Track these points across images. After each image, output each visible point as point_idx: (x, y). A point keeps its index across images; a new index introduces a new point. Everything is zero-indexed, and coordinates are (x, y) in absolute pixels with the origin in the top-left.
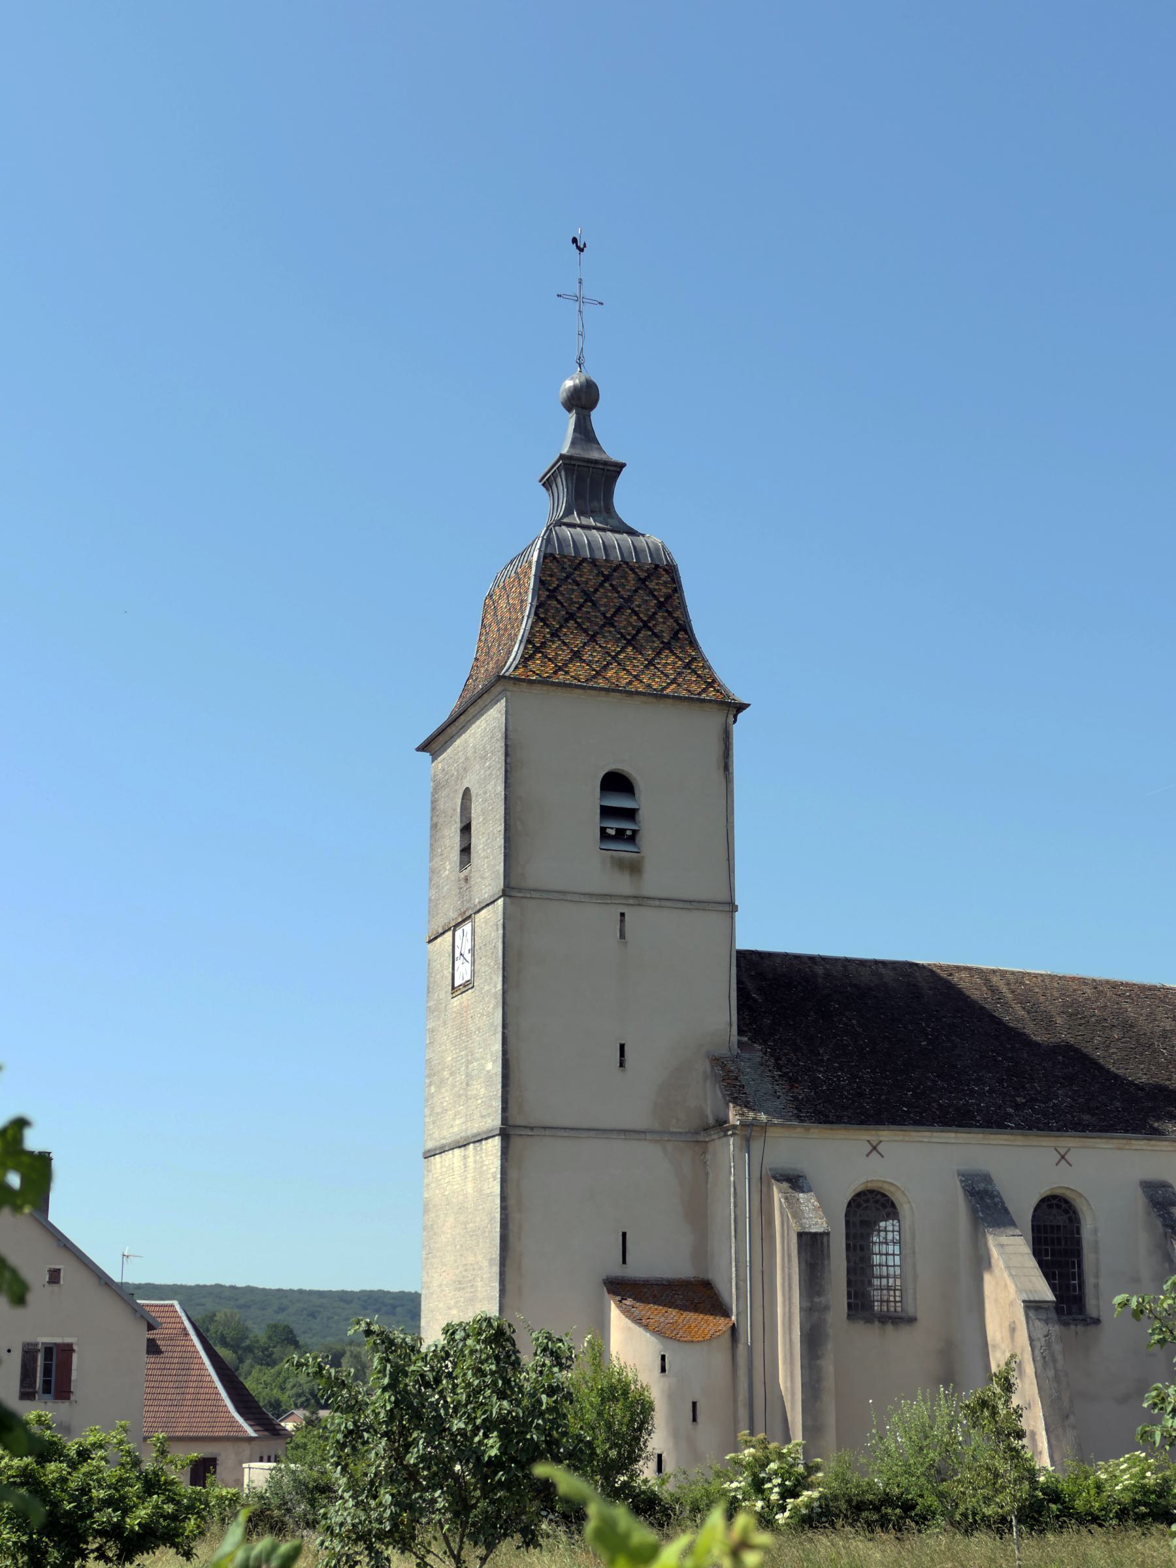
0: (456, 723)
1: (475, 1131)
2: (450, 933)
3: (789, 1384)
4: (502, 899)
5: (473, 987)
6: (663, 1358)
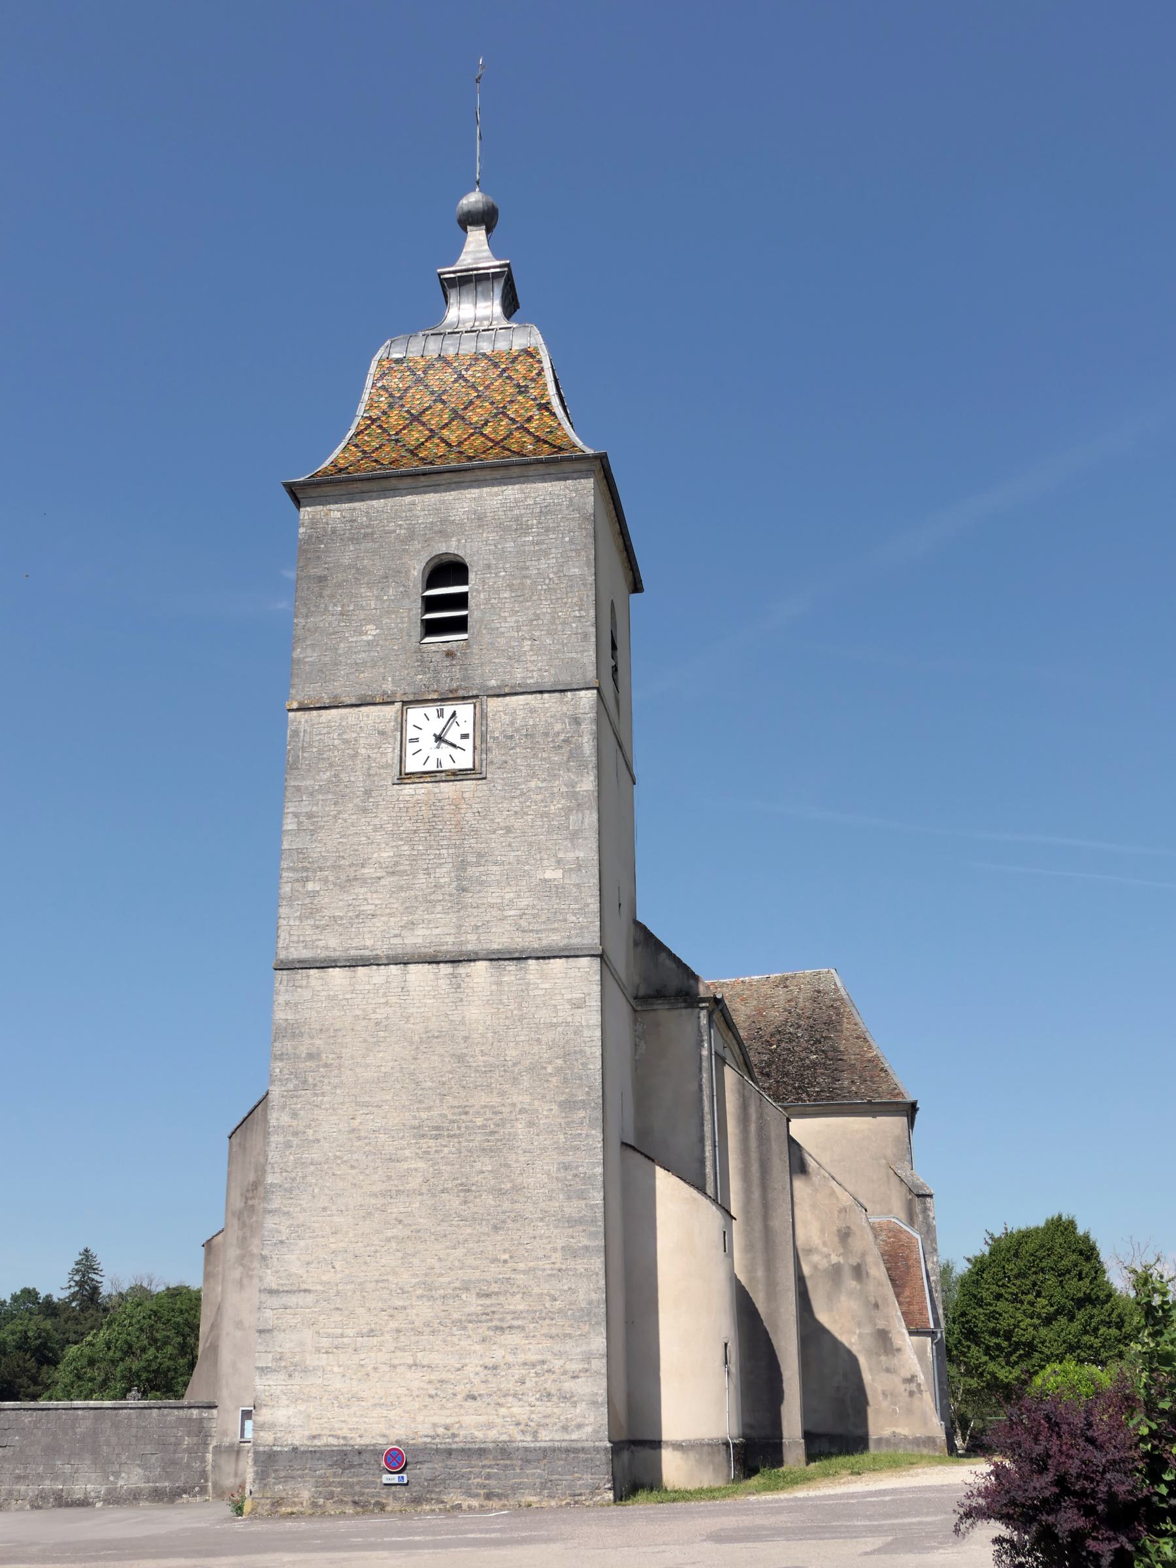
0: (422, 478)
1: (495, 946)
2: (391, 711)
3: (760, 1273)
4: (595, 691)
5: (485, 778)
6: (724, 1232)
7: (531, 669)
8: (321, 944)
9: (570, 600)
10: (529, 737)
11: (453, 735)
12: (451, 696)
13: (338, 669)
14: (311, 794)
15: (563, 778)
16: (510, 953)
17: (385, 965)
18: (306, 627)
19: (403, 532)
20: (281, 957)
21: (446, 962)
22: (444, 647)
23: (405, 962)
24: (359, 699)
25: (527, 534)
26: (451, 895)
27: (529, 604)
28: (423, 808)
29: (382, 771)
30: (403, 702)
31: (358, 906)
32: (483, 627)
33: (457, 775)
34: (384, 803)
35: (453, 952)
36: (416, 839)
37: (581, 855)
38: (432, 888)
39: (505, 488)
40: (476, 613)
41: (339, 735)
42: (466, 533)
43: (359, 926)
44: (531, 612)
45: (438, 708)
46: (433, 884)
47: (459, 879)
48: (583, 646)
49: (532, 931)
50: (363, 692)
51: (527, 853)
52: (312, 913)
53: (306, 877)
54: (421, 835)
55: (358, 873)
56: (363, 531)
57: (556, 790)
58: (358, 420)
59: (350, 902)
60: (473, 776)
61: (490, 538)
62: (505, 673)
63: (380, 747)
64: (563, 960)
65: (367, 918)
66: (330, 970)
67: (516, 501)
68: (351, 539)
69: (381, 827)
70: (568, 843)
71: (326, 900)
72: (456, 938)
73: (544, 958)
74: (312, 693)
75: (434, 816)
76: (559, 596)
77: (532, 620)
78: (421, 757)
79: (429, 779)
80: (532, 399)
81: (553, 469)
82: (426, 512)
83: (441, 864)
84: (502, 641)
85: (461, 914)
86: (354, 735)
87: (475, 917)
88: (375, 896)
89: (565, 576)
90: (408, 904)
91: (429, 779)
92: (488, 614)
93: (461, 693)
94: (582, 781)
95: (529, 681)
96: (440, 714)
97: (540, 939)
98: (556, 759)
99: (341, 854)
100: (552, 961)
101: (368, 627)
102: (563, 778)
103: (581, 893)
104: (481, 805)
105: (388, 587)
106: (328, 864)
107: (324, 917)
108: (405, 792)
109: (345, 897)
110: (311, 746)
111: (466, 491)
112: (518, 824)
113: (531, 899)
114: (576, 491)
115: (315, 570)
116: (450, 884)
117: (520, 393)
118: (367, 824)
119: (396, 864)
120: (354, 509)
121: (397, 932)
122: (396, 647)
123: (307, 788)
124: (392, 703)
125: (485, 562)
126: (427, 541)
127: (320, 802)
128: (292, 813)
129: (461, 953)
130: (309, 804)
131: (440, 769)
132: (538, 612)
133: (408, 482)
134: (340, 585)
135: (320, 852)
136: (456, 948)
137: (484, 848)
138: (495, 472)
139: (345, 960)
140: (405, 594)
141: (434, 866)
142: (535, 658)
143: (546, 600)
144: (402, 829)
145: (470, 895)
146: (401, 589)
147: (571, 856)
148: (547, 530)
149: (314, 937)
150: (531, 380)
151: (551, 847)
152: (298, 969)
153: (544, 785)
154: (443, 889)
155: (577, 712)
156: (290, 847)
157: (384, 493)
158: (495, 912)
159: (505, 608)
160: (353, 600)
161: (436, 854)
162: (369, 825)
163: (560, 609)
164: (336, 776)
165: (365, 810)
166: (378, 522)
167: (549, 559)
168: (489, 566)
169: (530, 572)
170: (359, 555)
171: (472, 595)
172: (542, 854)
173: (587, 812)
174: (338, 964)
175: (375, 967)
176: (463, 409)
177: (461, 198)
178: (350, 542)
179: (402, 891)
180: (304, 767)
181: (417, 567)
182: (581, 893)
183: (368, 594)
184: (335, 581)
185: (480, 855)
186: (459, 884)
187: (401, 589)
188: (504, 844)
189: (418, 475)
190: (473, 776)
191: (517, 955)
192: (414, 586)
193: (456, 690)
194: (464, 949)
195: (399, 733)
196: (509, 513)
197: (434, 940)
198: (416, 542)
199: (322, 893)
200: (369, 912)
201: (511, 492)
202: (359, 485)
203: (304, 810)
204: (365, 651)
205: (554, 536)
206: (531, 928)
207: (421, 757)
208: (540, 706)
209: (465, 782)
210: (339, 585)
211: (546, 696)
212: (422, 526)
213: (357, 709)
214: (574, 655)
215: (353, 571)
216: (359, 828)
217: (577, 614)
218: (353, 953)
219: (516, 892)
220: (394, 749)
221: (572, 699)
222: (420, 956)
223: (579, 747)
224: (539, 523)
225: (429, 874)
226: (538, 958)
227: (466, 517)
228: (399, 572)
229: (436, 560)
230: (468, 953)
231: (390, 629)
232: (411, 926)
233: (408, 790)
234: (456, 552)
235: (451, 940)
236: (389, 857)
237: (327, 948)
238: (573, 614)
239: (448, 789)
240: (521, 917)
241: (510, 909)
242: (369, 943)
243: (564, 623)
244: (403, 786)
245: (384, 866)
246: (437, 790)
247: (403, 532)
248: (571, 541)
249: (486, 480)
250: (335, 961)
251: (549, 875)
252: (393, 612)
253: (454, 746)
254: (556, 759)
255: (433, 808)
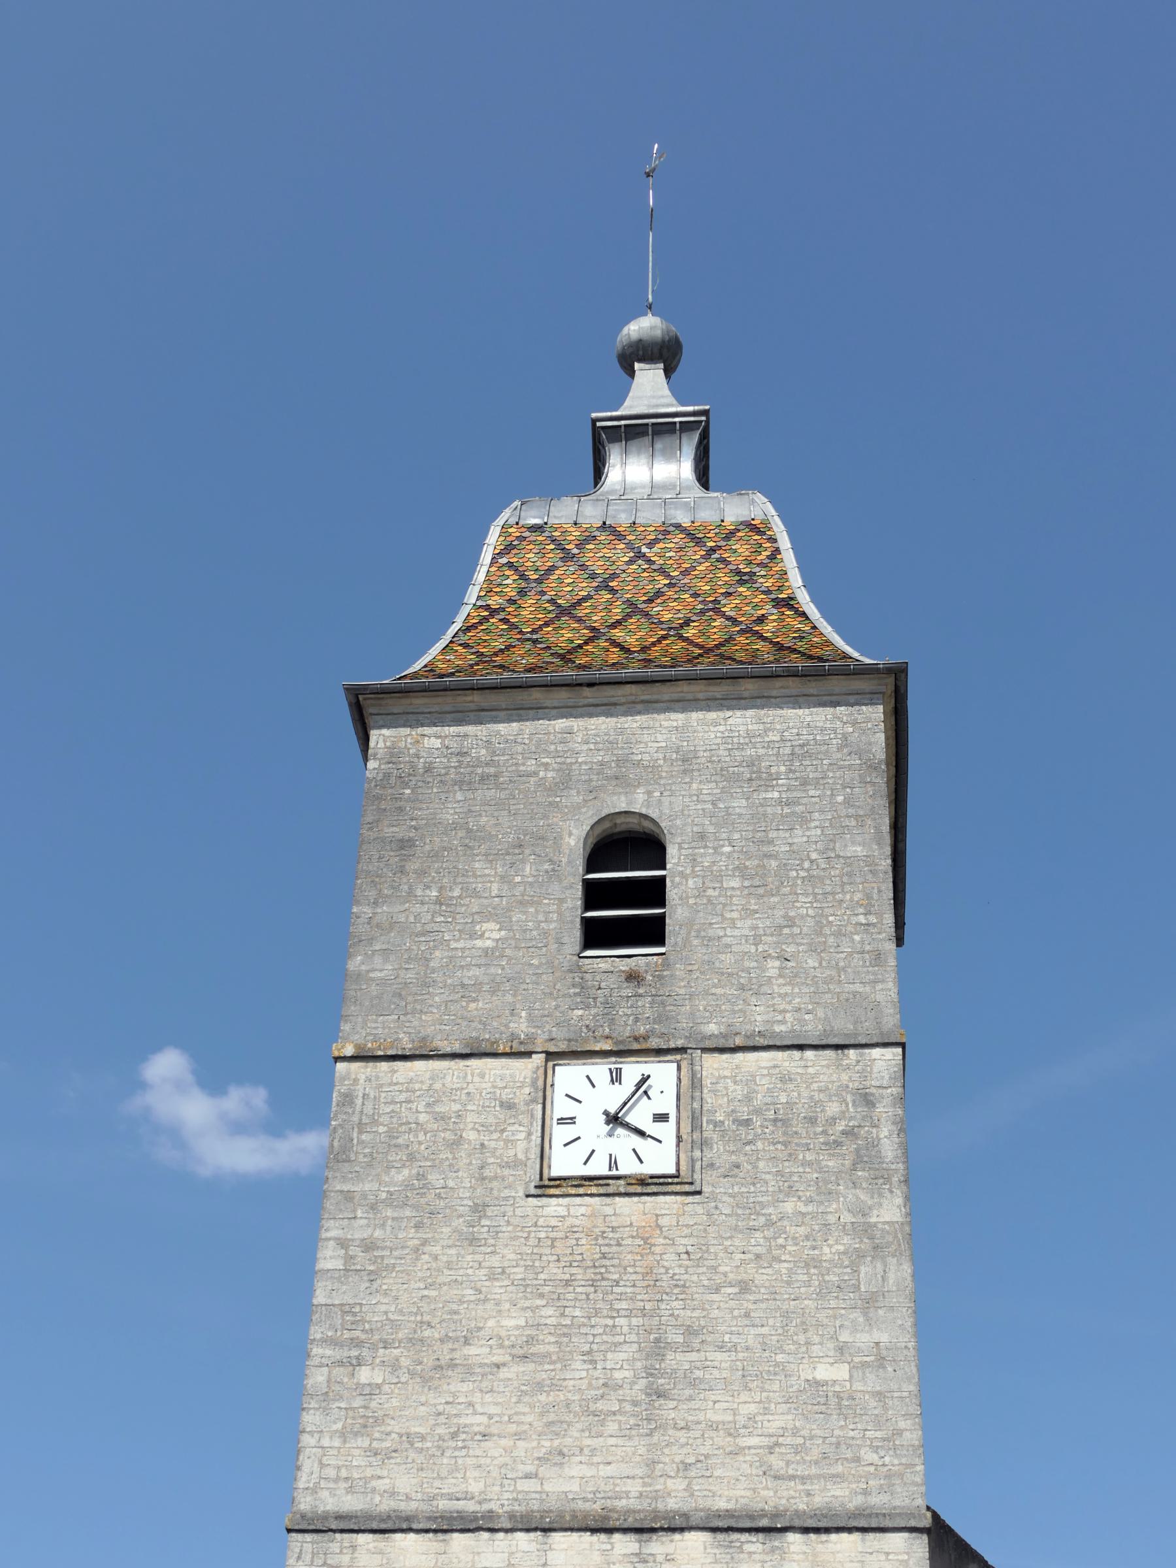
0: (587, 691)
1: (722, 1504)
2: (525, 1069)
4: (900, 1050)
5: (699, 1193)
7: (782, 1007)
8: (381, 1485)
9: (848, 897)
10: (779, 1124)
11: (639, 1116)
12: (636, 1046)
13: (428, 993)
14: (373, 1207)
15: (845, 1197)
16: (751, 1517)
17: (507, 1531)
18: (374, 922)
19: (550, 774)
20: (302, 1507)
21: (625, 1531)
22: (624, 965)
23: (547, 1526)
24: (467, 1045)
25: (769, 787)
26: (635, 1403)
27: (775, 899)
28: (583, 1241)
29: (506, 1172)
30: (550, 1056)
31: (456, 1415)
32: (693, 934)
33: (647, 1185)
34: (510, 1228)
35: (639, 1511)
36: (569, 1296)
37: (884, 1338)
38: (598, 1388)
39: (729, 713)
40: (679, 911)
41: (428, 1105)
42: (662, 782)
43: (457, 1453)
44: (779, 913)
45: (613, 1066)
46: (601, 1382)
47: (652, 1374)
48: (874, 974)
49: (792, 1478)
50: (474, 1034)
51: (780, 1331)
52: (365, 1426)
53: (357, 1358)
54: (579, 1290)
55: (457, 1355)
56: (479, 771)
57: (832, 1219)
58: (465, 610)
59: (440, 1408)
60: (678, 1188)
61: (705, 792)
62: (734, 1012)
63: (503, 1131)
64: (856, 1536)
65: (472, 1439)
66: (398, 1536)
67: (749, 735)
68: (460, 783)
69: (503, 1272)
70: (857, 1315)
71: (395, 1402)
72: (645, 1485)
73: (817, 1530)
74: (380, 1031)
75: (604, 1256)
76: (829, 889)
77: (781, 927)
78: (579, 1151)
79: (594, 1190)
80: (763, 592)
81: (812, 687)
82: (592, 746)
83: (616, 1345)
84: (728, 958)
85: (655, 1439)
86: (456, 1107)
87: (682, 1446)
88: (488, 1398)
89: (838, 856)
90: (552, 1417)
91: (594, 1190)
92: (701, 914)
93: (654, 1043)
94: (881, 1205)
95: (777, 1028)
96: (616, 1077)
97: (809, 1494)
98: (830, 1164)
99: (426, 1318)
100: (833, 1537)
101: (485, 926)
102: (845, 1197)
103: (885, 1408)
104: (692, 1241)
105: (523, 861)
106: (400, 1335)
107: (388, 1434)
108: (549, 1211)
109: (431, 1397)
110: (375, 1122)
111: (662, 716)
112: (763, 1277)
113: (790, 1417)
114: (854, 723)
115: (394, 829)
116: (633, 1383)
117: (741, 582)
118: (476, 1265)
119: (531, 1340)
120: (466, 735)
121: (530, 1468)
122: (535, 962)
123: (364, 1196)
124: (529, 1054)
125: (695, 829)
126: (593, 791)
127: (389, 1222)
128: (336, 1239)
129: (656, 1514)
130: (368, 1226)
131: (614, 1172)
132: (792, 914)
133: (563, 695)
134: (436, 856)
135: (386, 1313)
136: (645, 1505)
137: (698, 1318)
138: (711, 688)
139: (429, 1518)
140: (554, 874)
141: (603, 1348)
142: (788, 989)
143: (806, 895)
144: (542, 1276)
145: (672, 1404)
146: (546, 866)
147: (864, 1339)
148: (805, 783)
149: (369, 1472)
150: (758, 565)
151: (825, 1321)
152: (334, 1531)
153: (810, 1208)
154: (621, 1392)
155: (868, 1083)
156: (329, 1302)
157: (518, 713)
158: (721, 1439)
159: (731, 904)
160: (459, 880)
161: (606, 1326)
162: (480, 1267)
163: (831, 911)
164: (420, 1176)
165: (473, 1241)
166: (506, 757)
167: (808, 829)
168: (702, 836)
169: (776, 848)
170: (473, 808)
171: (672, 882)
172: (809, 1334)
173: (892, 1261)
174: (415, 1526)
175: (485, 1535)
176: (644, 602)
177: (628, 322)
178: (456, 788)
179: (541, 1391)
180: (361, 1158)
181: (574, 831)
182: (885, 1408)
183: (487, 872)
184: (427, 848)
185: (690, 1331)
186: (651, 1384)
187: (546, 866)
188: (736, 1313)
189: (580, 685)
190: (678, 1188)
191: (764, 1523)
192: (569, 862)
193: (646, 1038)
194: (660, 1506)
195: (540, 1107)
196: (737, 753)
197: (603, 1487)
198: (574, 792)
199: (386, 1388)
200: (476, 1429)
201: (741, 720)
202: (476, 697)
203: (358, 1235)
204: (479, 966)
205: (818, 793)
206: (791, 1472)
207: (579, 1151)
208: (800, 1070)
209: (661, 1198)
210: (435, 855)
211: (809, 1054)
212: (584, 767)
213: (462, 1063)
214: (858, 987)
215: (461, 834)
216: (461, 1272)
217: (862, 919)
218: (443, 1505)
219: (760, 1402)
220: (530, 1134)
221: (858, 1062)
222: (574, 1517)
223: (874, 1144)
224: (791, 771)
225: (595, 1362)
226: (806, 1530)
227: (661, 756)
228: (542, 838)
229: (607, 825)
230: (667, 1515)
231: (525, 931)
232: (558, 1459)
233: (554, 1207)
234: (644, 811)
235: (634, 1487)
236: (518, 1327)
237: (393, 1494)
238: (854, 920)
239: (628, 1208)
240: (771, 1449)
241: (750, 1434)
242: (475, 1487)
243: (839, 934)
244: (545, 1200)
245: (507, 1343)
246: (608, 1210)
247: (550, 774)
248: (847, 802)
249: (696, 700)
250: (408, 1519)
251: (823, 1372)
252: (532, 903)
253: (641, 1133)
254: (830, 1164)
255: (600, 1241)
